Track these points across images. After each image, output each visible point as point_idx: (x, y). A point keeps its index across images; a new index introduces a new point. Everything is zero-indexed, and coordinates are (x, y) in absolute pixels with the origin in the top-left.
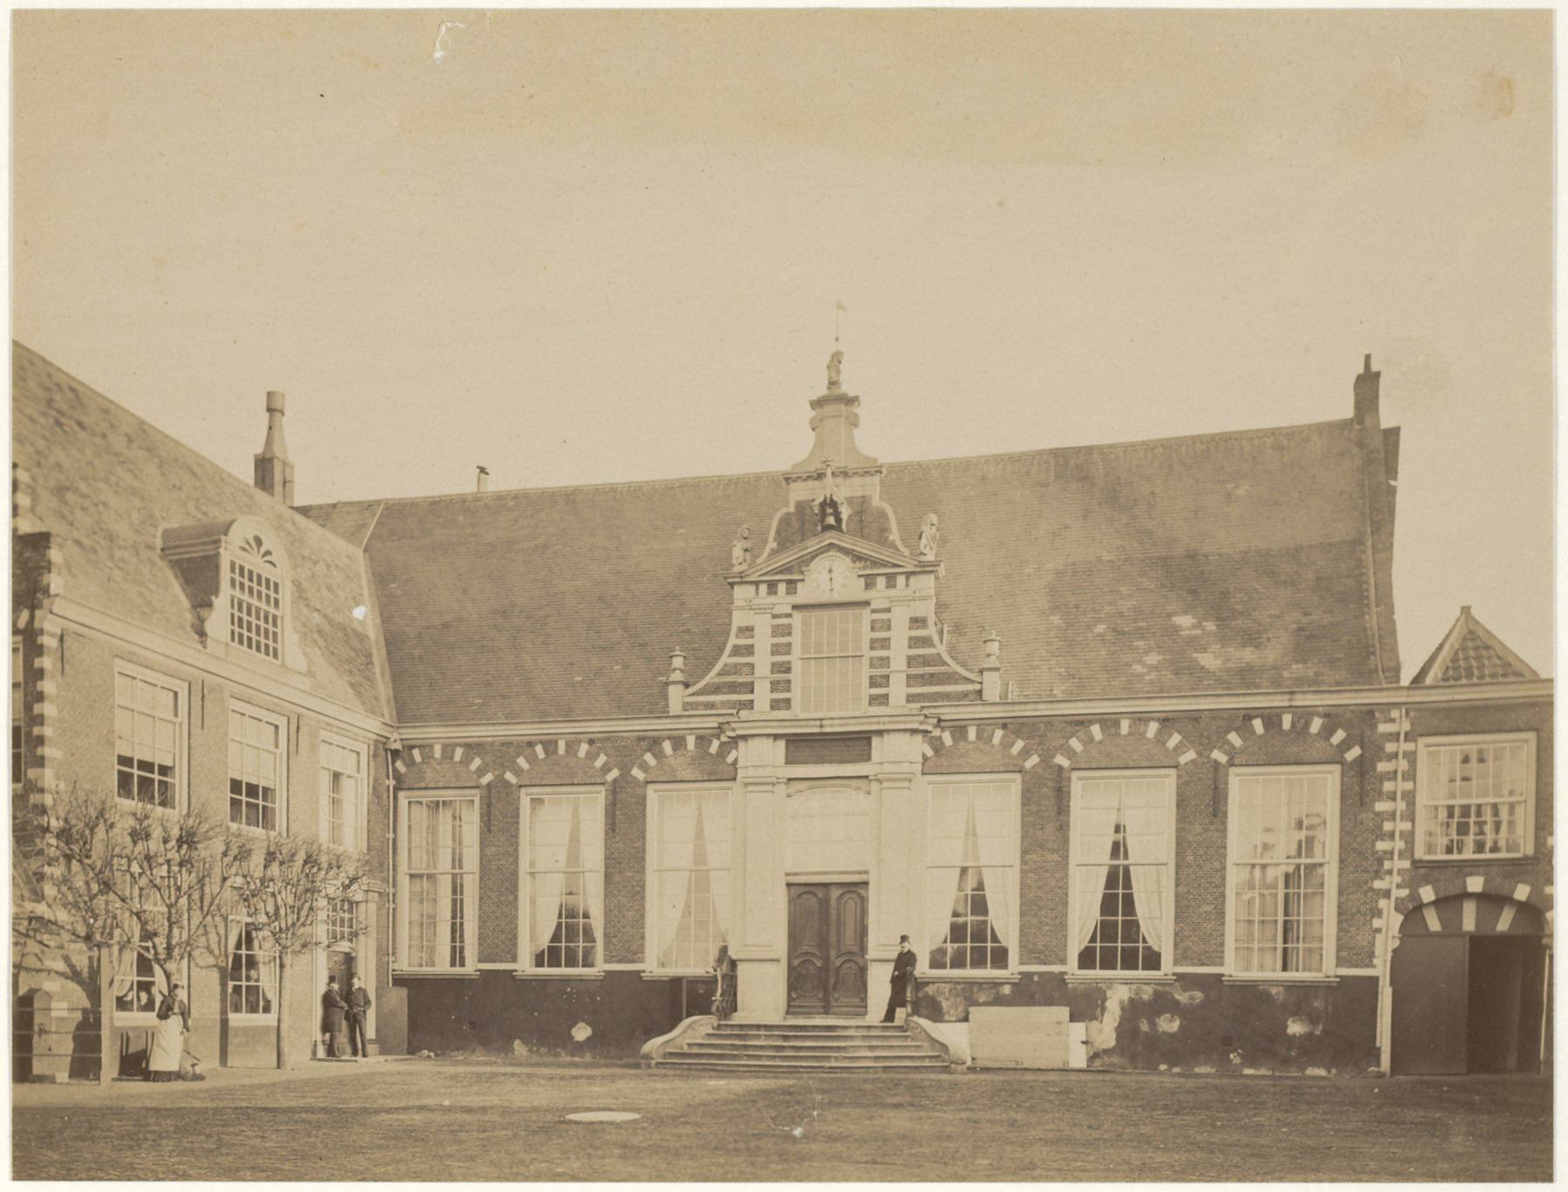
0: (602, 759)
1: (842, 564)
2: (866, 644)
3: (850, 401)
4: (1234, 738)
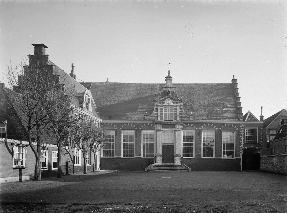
0: (135, 126)
1: (170, 100)
2: (173, 111)
3: (172, 77)
4: (222, 127)
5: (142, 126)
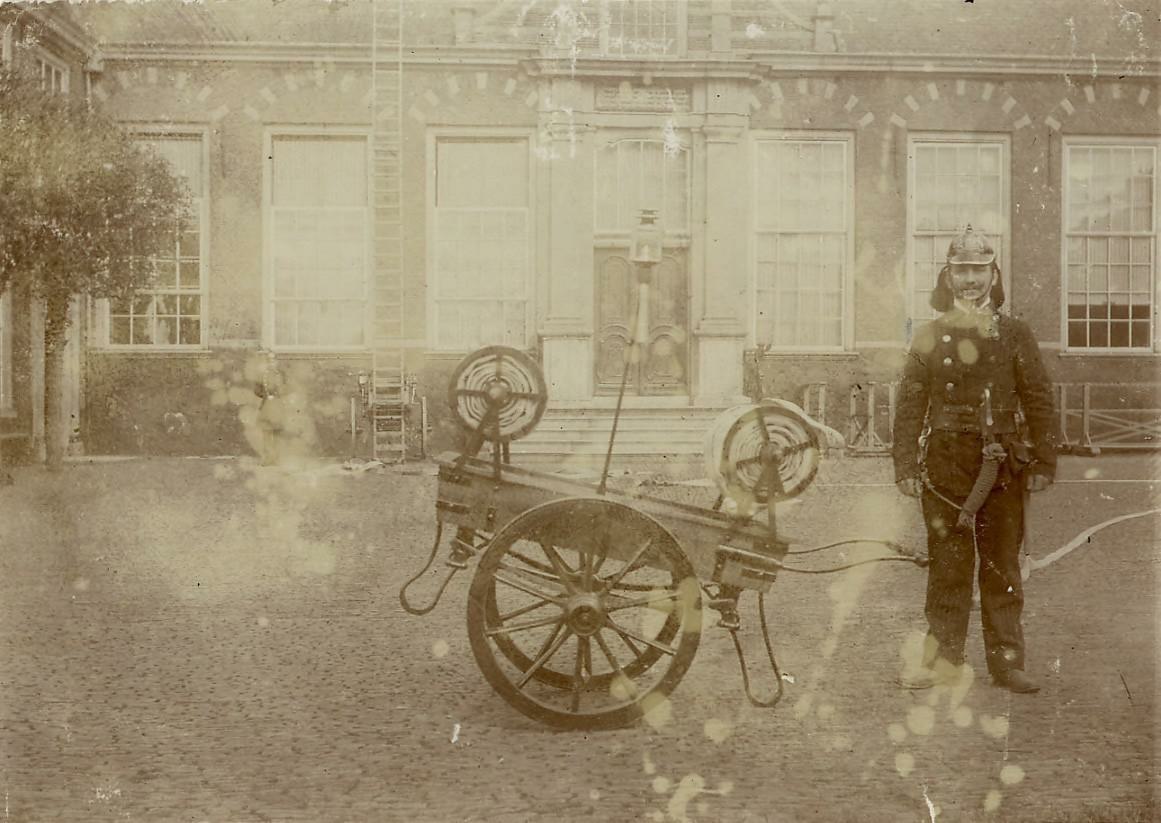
5: (432, 98)
